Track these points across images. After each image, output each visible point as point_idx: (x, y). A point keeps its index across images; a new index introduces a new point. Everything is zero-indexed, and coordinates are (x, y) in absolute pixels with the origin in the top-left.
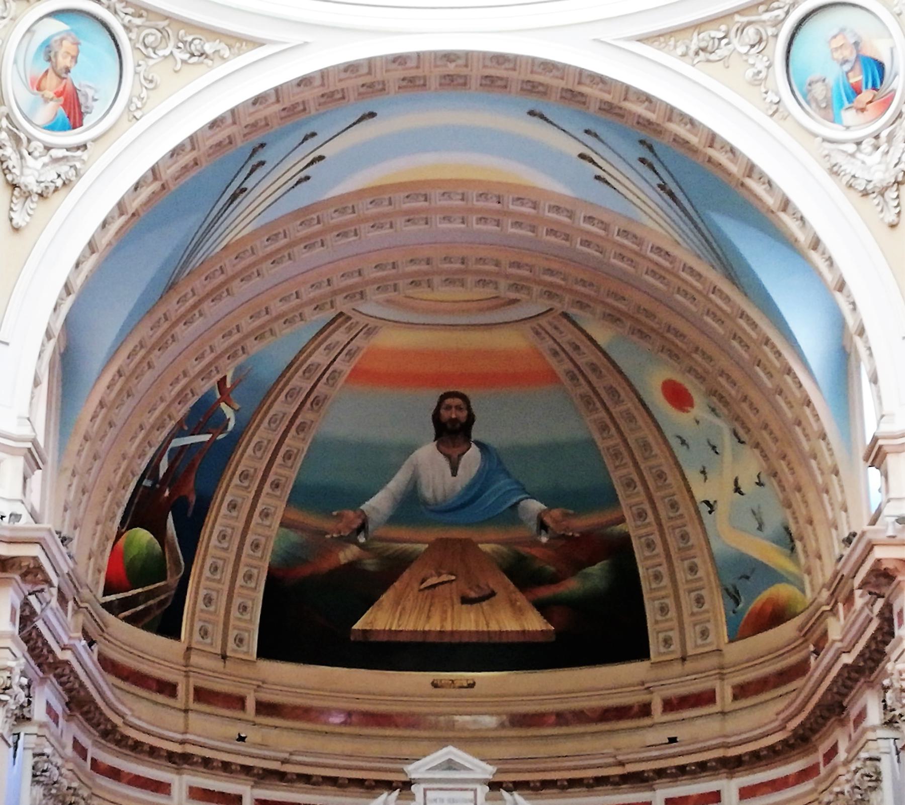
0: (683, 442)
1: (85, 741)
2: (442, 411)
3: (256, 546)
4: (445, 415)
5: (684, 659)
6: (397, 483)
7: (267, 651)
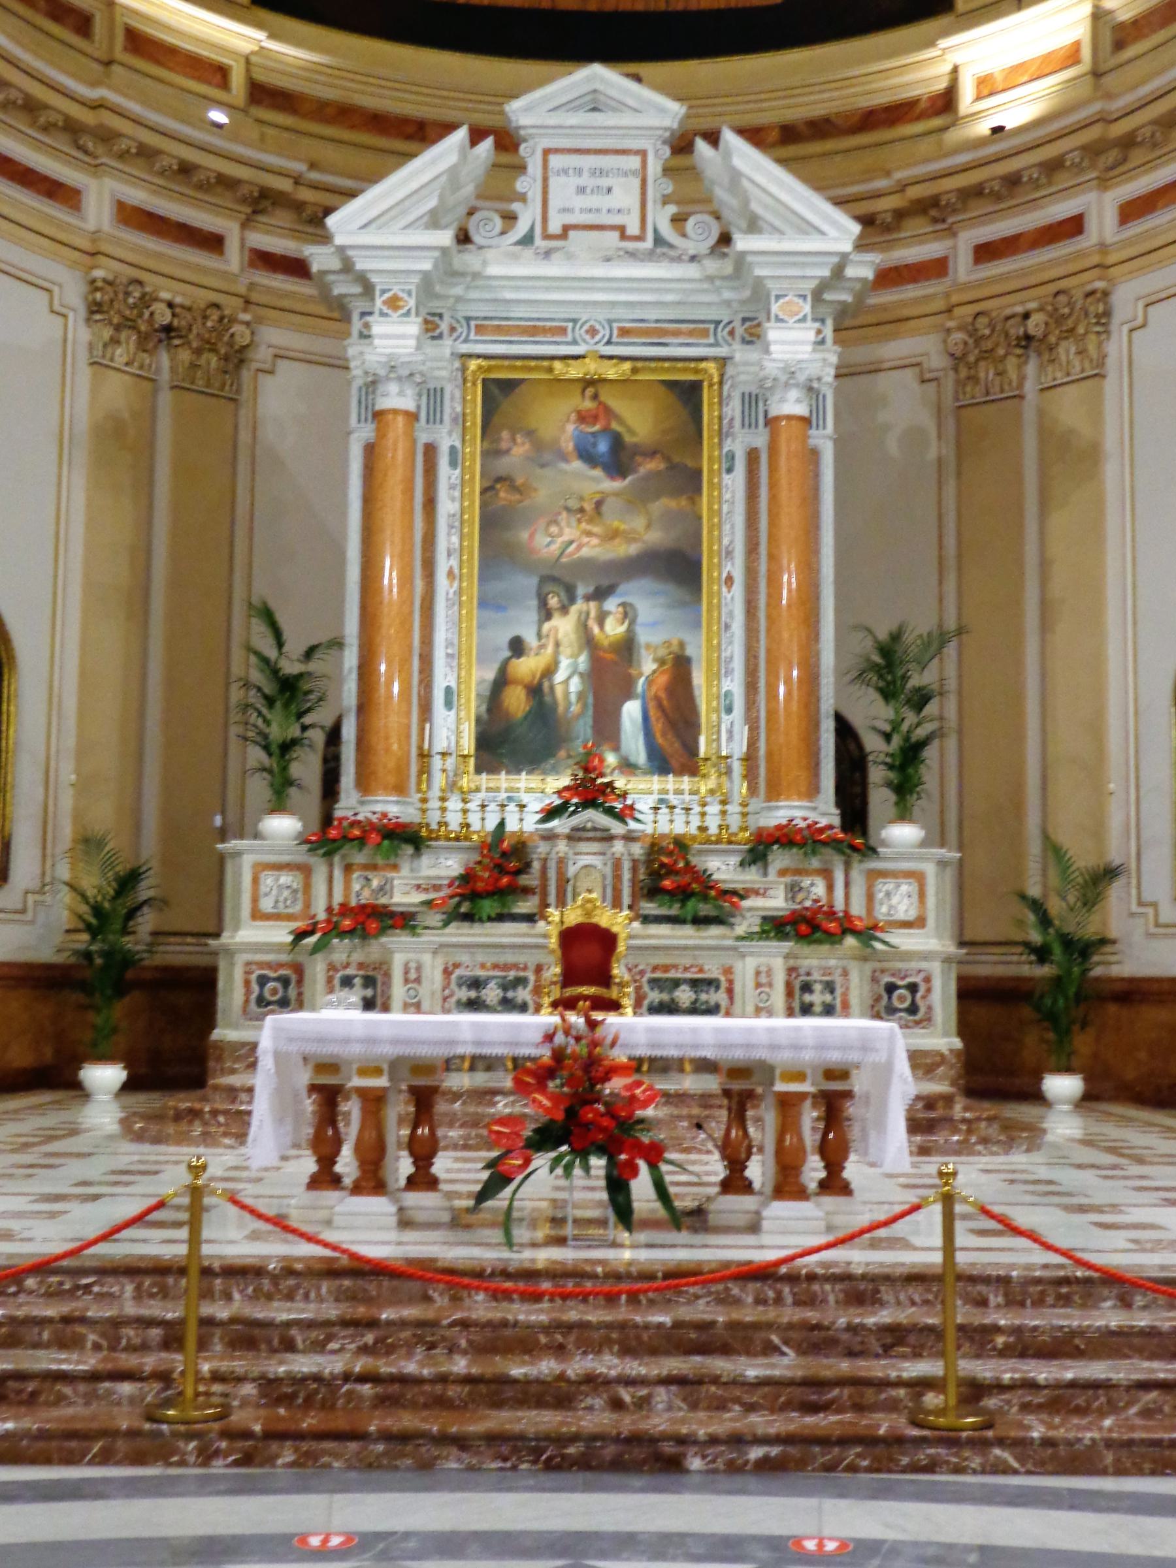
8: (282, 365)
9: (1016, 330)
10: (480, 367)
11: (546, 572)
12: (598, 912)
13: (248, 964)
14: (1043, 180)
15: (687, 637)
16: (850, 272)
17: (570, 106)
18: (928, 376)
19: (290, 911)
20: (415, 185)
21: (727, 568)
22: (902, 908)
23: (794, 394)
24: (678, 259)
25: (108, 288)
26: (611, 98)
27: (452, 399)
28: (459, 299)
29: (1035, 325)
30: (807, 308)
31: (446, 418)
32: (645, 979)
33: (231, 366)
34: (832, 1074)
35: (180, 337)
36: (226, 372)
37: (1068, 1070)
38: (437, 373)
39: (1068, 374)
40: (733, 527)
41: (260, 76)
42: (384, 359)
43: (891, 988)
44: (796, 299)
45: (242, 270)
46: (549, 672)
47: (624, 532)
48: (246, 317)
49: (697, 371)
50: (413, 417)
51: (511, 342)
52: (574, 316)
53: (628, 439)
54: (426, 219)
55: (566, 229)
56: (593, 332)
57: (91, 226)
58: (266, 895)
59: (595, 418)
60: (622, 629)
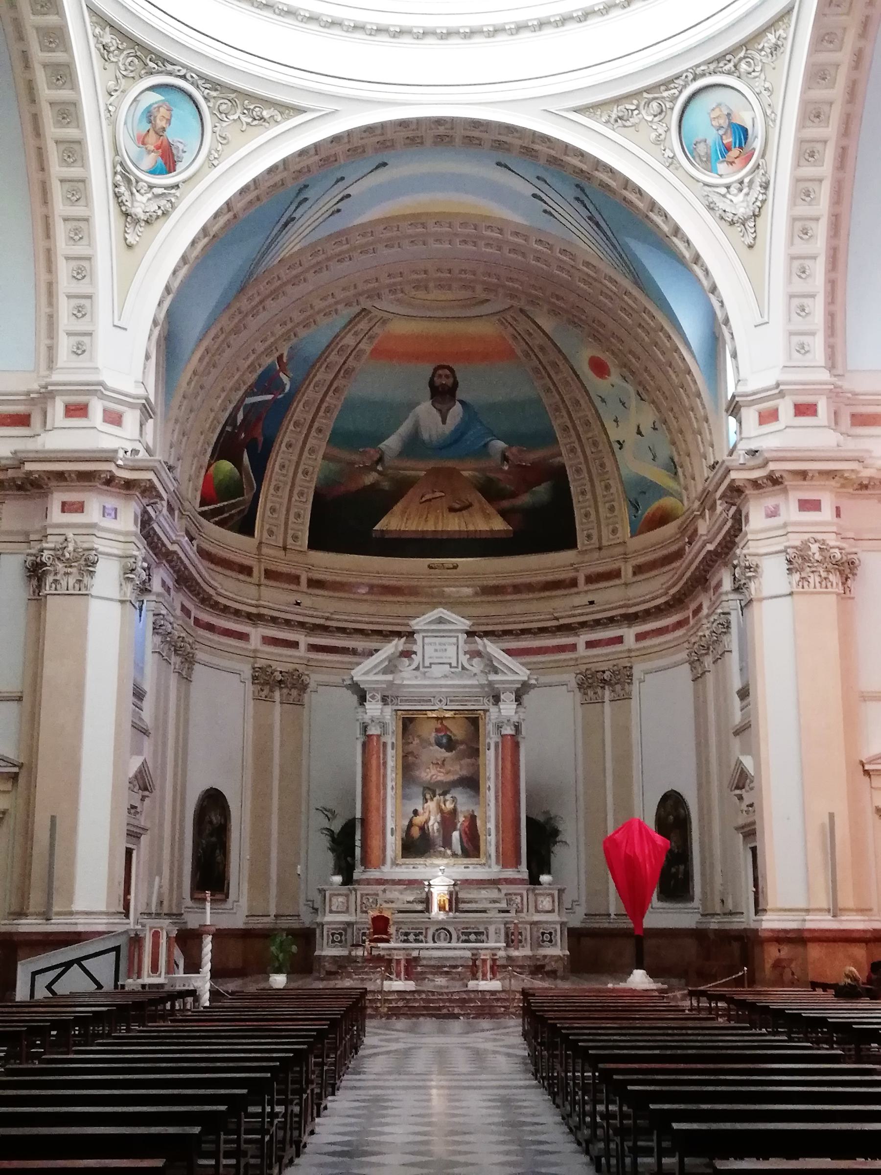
0: (603, 401)
1: (189, 605)
2: (435, 379)
3: (306, 473)
4: (438, 381)
5: (600, 549)
6: (404, 429)
7: (315, 544)
8: (320, 689)
9: (599, 675)
21: (488, 784)
29: (606, 676)
43: (543, 934)
46: (427, 822)
55: (431, 664)
56: (441, 701)
57: (252, 647)
60: (452, 806)
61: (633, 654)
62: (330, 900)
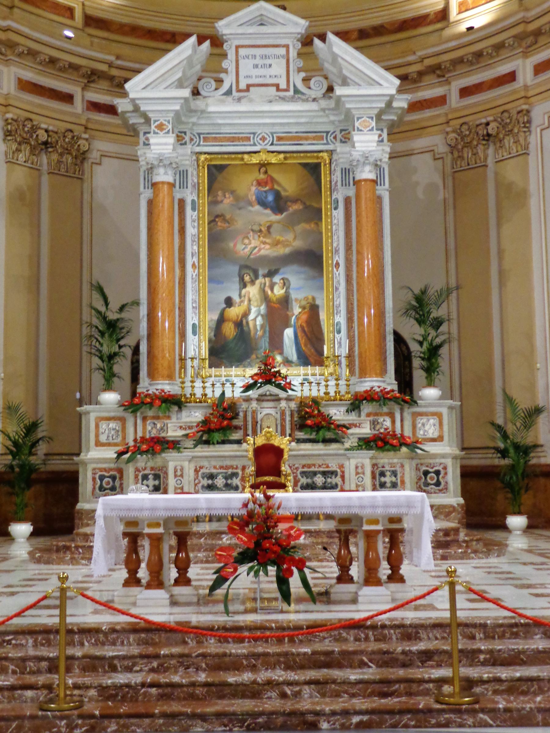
8: (105, 160)
9: (482, 131)
10: (206, 159)
11: (243, 263)
12: (273, 438)
13: (94, 469)
14: (494, 54)
15: (316, 295)
16: (395, 104)
17: (250, 23)
18: (437, 156)
19: (115, 441)
20: (170, 66)
21: (336, 258)
22: (431, 431)
23: (368, 168)
24: (307, 100)
25: (14, 123)
26: (269, 18)
27: (192, 176)
28: (194, 124)
29: (492, 128)
30: (374, 124)
31: (189, 185)
32: (298, 472)
33: (78, 162)
34: (392, 520)
35: (52, 147)
36: (76, 165)
37: (519, 513)
38: (184, 162)
39: (510, 153)
40: (338, 237)
41: (89, 12)
42: (156, 156)
43: (426, 473)
44: (368, 119)
45: (83, 111)
46: (246, 314)
47: (283, 241)
48: (86, 136)
49: (318, 158)
50: (172, 185)
51: (222, 145)
52: (254, 131)
53: (283, 193)
54: (176, 83)
55: (249, 86)
56: (263, 139)
58: (103, 433)
59: (266, 184)
60: (282, 292)
61: (530, 93)
62: (97, 426)
